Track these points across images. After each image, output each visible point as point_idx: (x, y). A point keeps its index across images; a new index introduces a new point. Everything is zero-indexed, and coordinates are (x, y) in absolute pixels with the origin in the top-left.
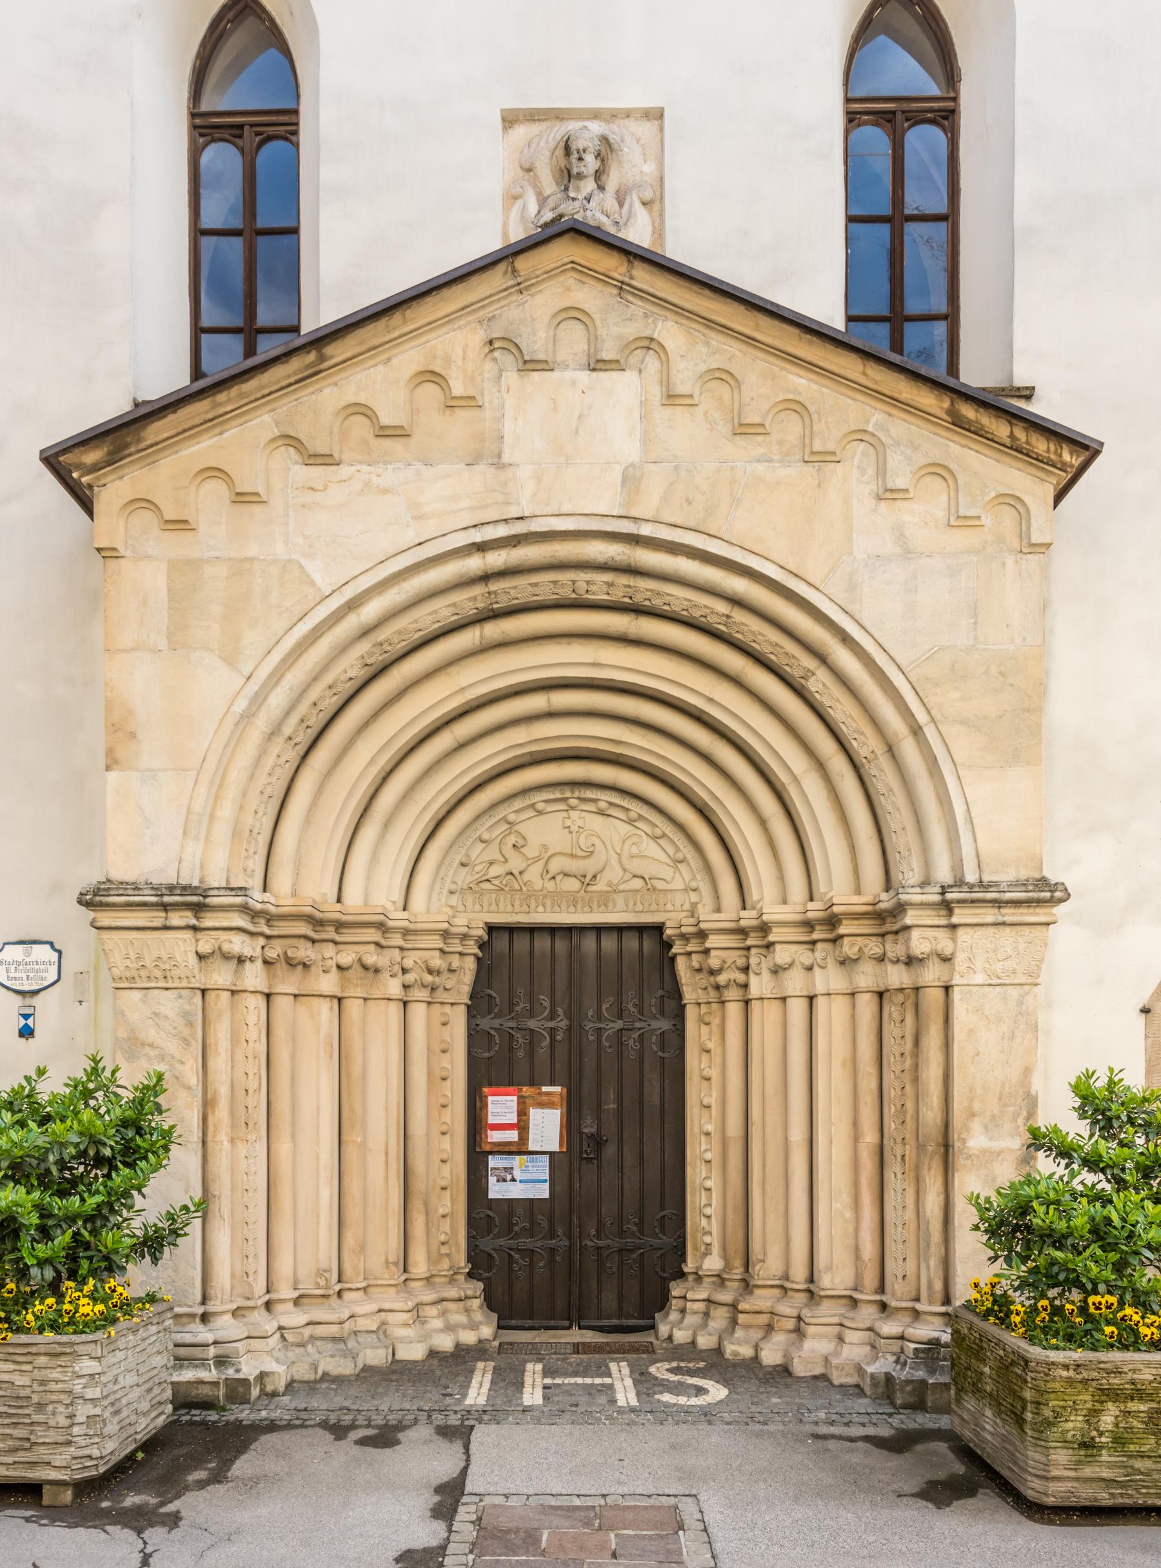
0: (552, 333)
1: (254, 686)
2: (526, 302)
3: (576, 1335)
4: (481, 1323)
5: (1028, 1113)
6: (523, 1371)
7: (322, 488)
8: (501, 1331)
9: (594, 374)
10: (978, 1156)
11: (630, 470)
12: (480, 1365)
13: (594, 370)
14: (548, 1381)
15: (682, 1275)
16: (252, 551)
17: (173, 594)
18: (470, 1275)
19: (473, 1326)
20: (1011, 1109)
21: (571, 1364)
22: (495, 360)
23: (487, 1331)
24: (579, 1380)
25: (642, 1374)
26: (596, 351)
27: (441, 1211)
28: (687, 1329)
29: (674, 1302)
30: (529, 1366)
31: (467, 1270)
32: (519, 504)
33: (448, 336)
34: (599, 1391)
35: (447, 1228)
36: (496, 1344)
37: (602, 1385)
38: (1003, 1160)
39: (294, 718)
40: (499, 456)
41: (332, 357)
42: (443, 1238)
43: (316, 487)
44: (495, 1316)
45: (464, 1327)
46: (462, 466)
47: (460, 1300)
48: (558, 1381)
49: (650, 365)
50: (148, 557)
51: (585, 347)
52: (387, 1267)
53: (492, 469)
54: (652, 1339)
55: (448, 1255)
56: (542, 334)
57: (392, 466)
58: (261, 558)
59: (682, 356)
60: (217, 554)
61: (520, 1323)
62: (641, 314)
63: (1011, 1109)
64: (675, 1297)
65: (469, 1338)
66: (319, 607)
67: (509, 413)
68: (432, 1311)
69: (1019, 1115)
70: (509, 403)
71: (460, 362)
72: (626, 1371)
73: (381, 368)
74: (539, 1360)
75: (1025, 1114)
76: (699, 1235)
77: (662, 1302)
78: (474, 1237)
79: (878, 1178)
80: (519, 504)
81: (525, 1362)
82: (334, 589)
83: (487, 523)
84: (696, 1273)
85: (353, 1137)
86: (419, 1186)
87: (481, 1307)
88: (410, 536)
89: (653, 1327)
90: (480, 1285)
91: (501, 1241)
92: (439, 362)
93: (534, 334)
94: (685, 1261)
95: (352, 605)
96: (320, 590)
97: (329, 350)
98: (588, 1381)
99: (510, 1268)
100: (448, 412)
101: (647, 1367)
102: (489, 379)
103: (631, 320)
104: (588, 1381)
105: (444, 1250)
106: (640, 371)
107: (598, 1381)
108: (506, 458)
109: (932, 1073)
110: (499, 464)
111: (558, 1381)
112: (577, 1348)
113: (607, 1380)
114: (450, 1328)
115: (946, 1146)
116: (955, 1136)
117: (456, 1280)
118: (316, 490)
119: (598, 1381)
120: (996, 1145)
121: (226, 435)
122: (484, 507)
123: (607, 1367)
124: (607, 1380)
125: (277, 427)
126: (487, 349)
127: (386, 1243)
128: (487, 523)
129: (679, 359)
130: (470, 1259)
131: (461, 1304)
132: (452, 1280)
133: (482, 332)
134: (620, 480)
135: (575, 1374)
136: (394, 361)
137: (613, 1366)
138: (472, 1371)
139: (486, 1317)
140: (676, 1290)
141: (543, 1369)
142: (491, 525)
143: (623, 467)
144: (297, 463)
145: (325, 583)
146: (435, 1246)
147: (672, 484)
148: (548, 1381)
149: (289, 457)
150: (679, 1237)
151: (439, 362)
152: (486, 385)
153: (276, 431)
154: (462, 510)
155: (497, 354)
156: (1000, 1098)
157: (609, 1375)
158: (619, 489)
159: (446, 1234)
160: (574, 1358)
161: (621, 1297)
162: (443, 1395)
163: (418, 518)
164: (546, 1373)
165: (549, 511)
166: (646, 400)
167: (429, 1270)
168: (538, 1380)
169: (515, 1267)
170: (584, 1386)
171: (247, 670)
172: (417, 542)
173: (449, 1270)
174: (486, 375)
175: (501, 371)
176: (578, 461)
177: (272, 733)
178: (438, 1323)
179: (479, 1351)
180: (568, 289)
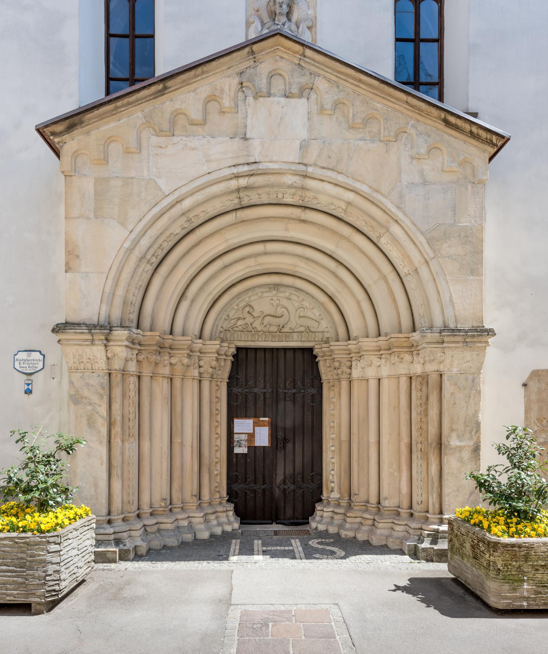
0: (269, 80)
1: (133, 236)
2: (258, 66)
3: (275, 527)
4: (233, 522)
5: (476, 429)
6: (253, 544)
7: (165, 147)
8: (242, 525)
9: (288, 100)
10: (455, 449)
11: (304, 142)
12: (234, 541)
13: (288, 97)
14: (264, 548)
15: (320, 500)
16: (133, 174)
17: (96, 193)
18: (228, 501)
19: (230, 523)
20: (469, 428)
21: (274, 541)
22: (243, 92)
23: (236, 525)
24: (278, 548)
25: (306, 545)
26: (290, 89)
27: (216, 472)
28: (325, 524)
29: (318, 512)
30: (256, 542)
31: (227, 499)
32: (254, 156)
33: (222, 80)
34: (288, 553)
35: (218, 480)
36: (240, 531)
37: (289, 550)
38: (465, 450)
39: (152, 251)
40: (245, 134)
41: (170, 88)
42: (216, 485)
43: (162, 146)
44: (239, 518)
45: (226, 524)
46: (228, 138)
47: (224, 512)
48: (269, 548)
49: (312, 96)
50: (85, 175)
51: (284, 87)
52: (192, 497)
53: (242, 140)
54: (308, 529)
55: (218, 492)
56: (264, 81)
57: (197, 138)
58: (137, 177)
59: (326, 92)
60: (117, 175)
61: (250, 521)
62: (309, 73)
63: (469, 428)
64: (318, 510)
65: (228, 528)
66: (163, 200)
67: (250, 115)
68: (212, 517)
69: (472, 430)
70: (250, 111)
71: (227, 91)
72: (299, 543)
73: (192, 94)
74: (260, 539)
75: (475, 430)
76: (329, 483)
77: (312, 511)
78: (230, 484)
79: (410, 458)
80: (254, 156)
81: (254, 539)
82: (170, 192)
83: (240, 165)
84: (327, 500)
85: (177, 440)
86: (206, 461)
87: (233, 515)
88: (205, 169)
89: (308, 523)
90: (233, 505)
91: (242, 486)
92: (218, 91)
93: (261, 80)
94: (322, 494)
95: (179, 201)
96: (164, 192)
97: (169, 83)
98: (282, 548)
99: (246, 498)
100: (222, 115)
101: (308, 541)
102: (241, 100)
103: (304, 75)
104: (282, 548)
105: (217, 490)
106: (308, 99)
107: (287, 548)
108: (248, 136)
109: (433, 413)
110: (245, 139)
111: (269, 548)
112: (276, 533)
113: (291, 548)
114: (219, 524)
115: (440, 444)
116: (444, 440)
117: (222, 503)
118: (162, 148)
119: (287, 548)
120: (462, 444)
121: (121, 121)
122: (238, 157)
123: (290, 541)
124: (291, 548)
125: (145, 118)
126: (240, 86)
127: (191, 486)
128: (240, 165)
129: (325, 94)
130: (228, 494)
131: (225, 514)
132: (220, 503)
133: (238, 79)
134: (299, 147)
135: (277, 545)
136: (198, 90)
137: (293, 541)
138: (230, 544)
139: (235, 519)
140: (318, 507)
141: (262, 543)
142: (241, 165)
143: (300, 141)
144: (153, 135)
145: (166, 189)
146: (213, 488)
147: (322, 149)
148: (264, 548)
149: (150, 132)
150: (319, 484)
151: (218, 91)
152: (239, 102)
153: (144, 120)
154: (228, 158)
155: (244, 89)
156: (464, 423)
157: (292, 545)
158: (299, 151)
159: (218, 482)
160: (275, 538)
161: (294, 509)
162: (218, 555)
163: (208, 161)
164: (263, 545)
165: (266, 159)
166: (311, 111)
167: (210, 499)
168: (260, 548)
169: (248, 497)
170: (280, 551)
171: (130, 228)
172: (208, 172)
173: (219, 499)
174: (239, 98)
175: (246, 97)
176: (280, 138)
177: (141, 258)
178: (215, 522)
179: (232, 535)
180: (276, 61)
